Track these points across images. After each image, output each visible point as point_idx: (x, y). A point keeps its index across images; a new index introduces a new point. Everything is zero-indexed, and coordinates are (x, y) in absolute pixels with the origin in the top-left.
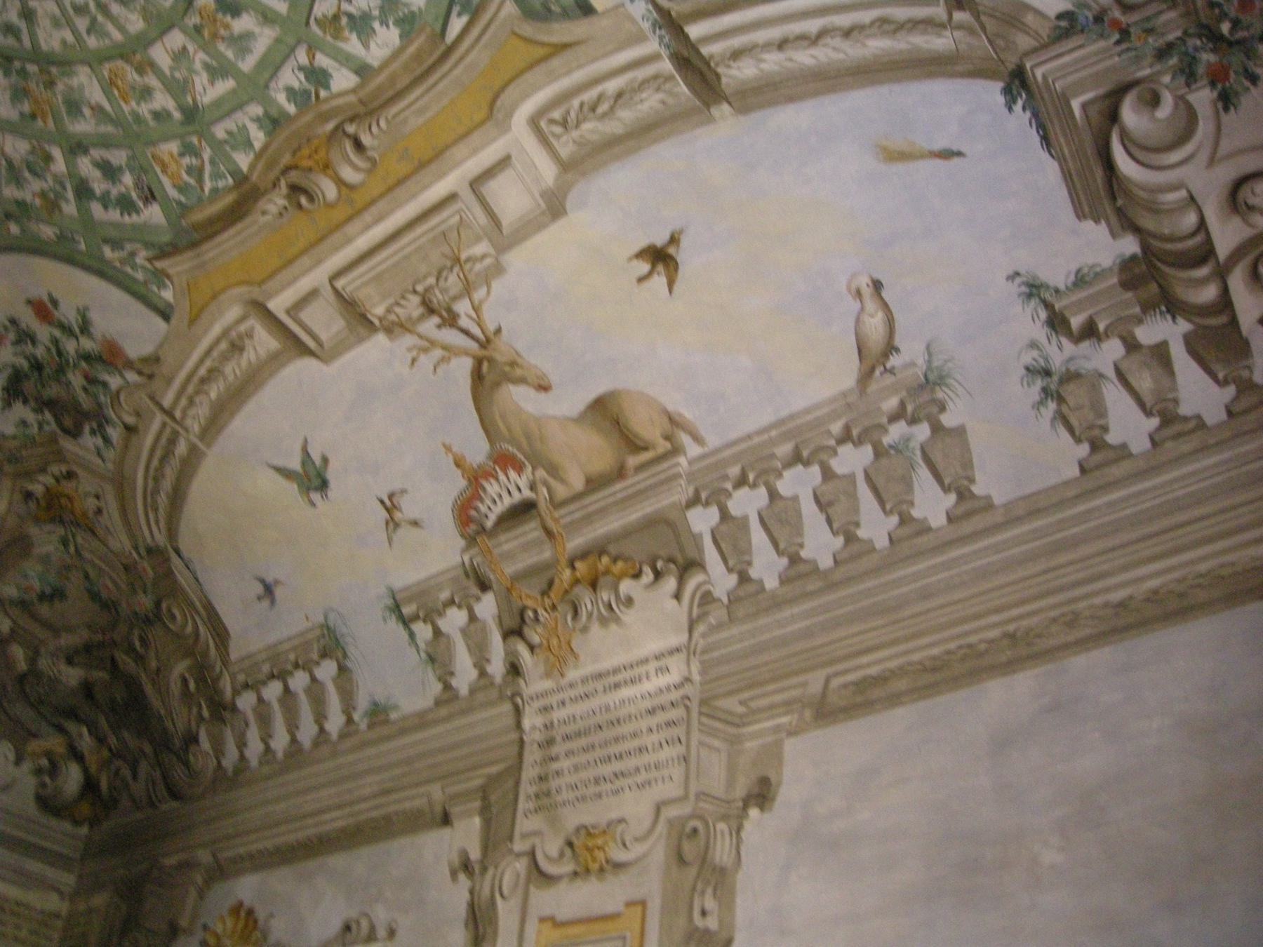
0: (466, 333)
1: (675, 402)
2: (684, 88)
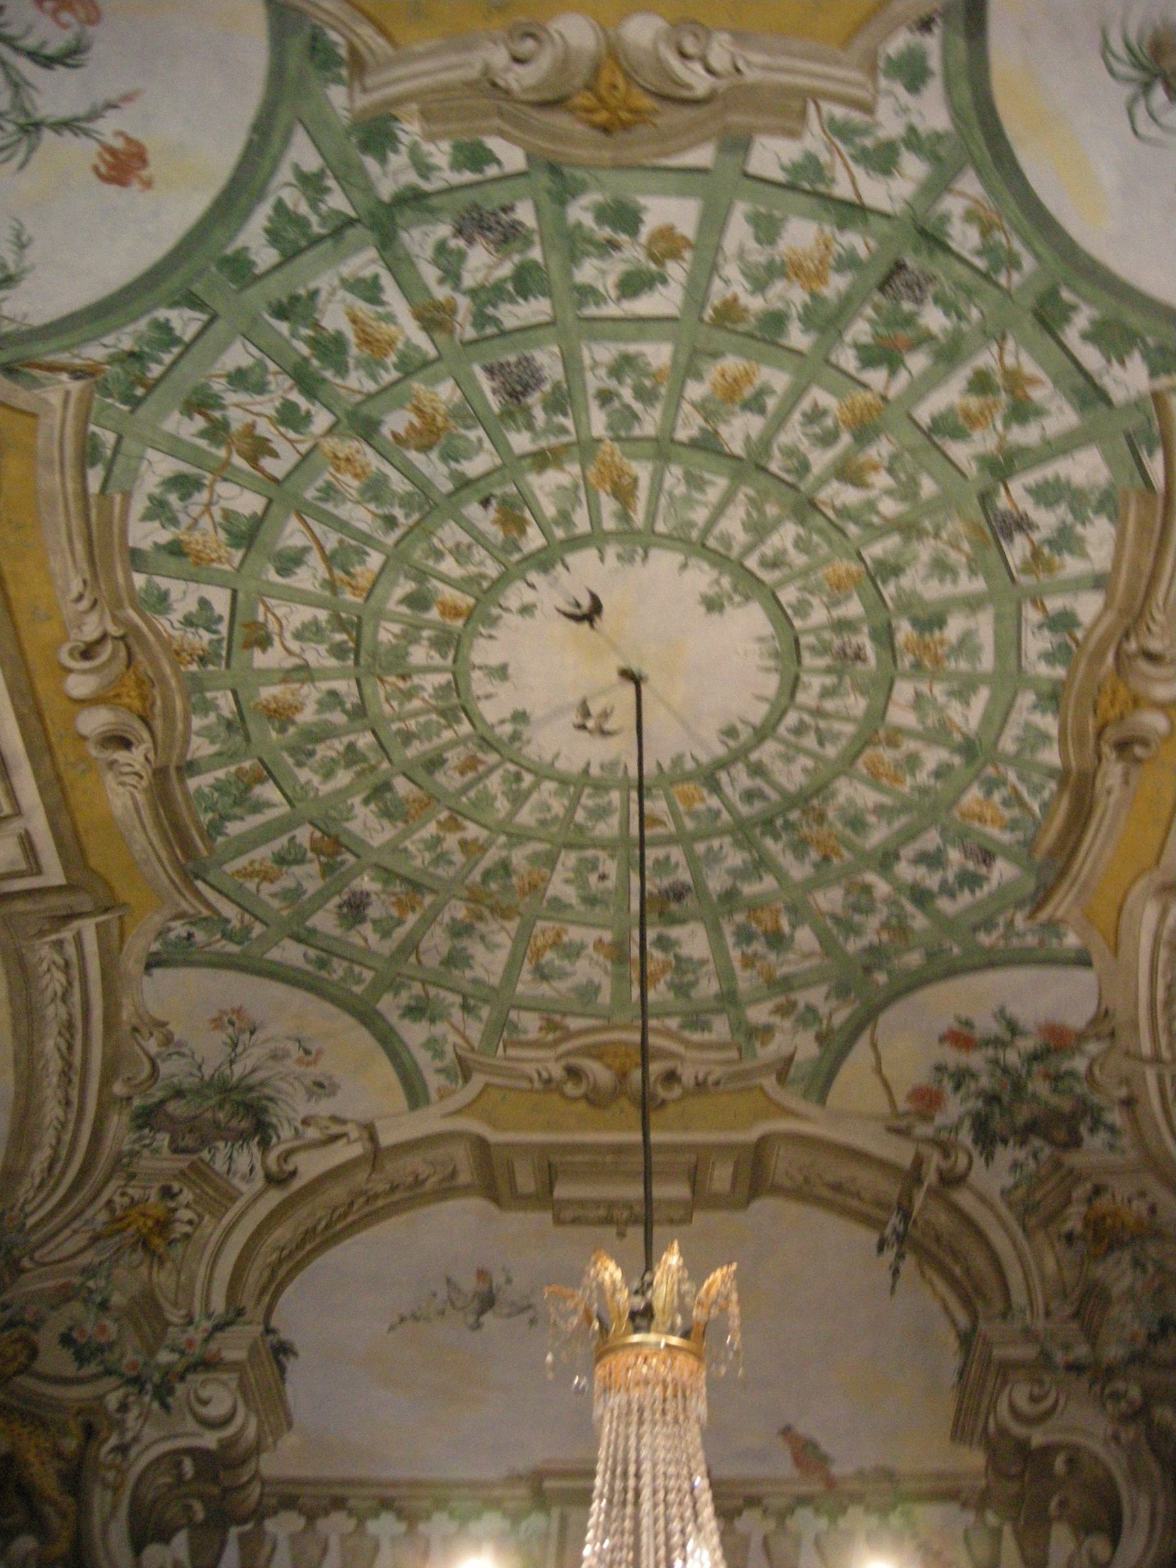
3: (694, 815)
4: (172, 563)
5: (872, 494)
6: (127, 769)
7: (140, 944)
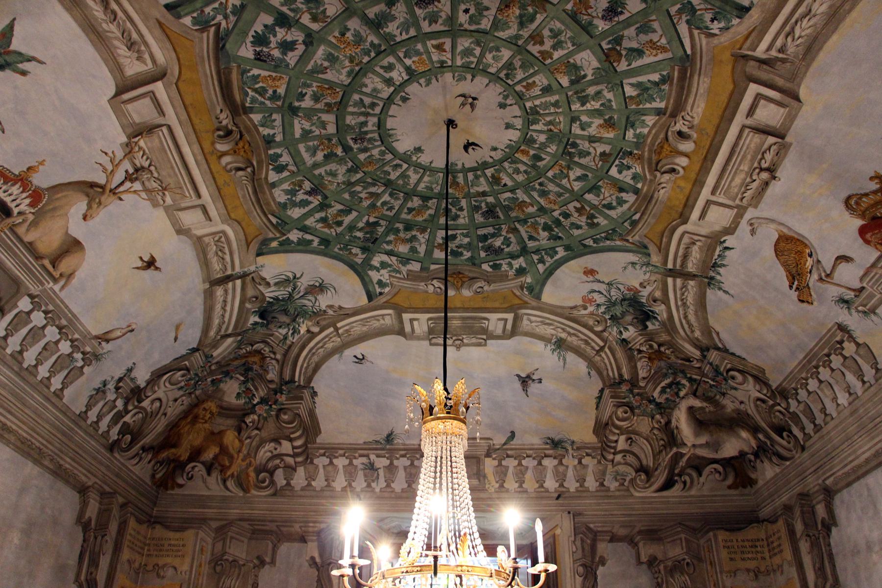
0: (122, 183)
1: (80, 275)
2: (219, 276)
3: (418, 53)
4: (625, 186)
5: (365, 191)
6: (686, 123)
7: (740, 27)
